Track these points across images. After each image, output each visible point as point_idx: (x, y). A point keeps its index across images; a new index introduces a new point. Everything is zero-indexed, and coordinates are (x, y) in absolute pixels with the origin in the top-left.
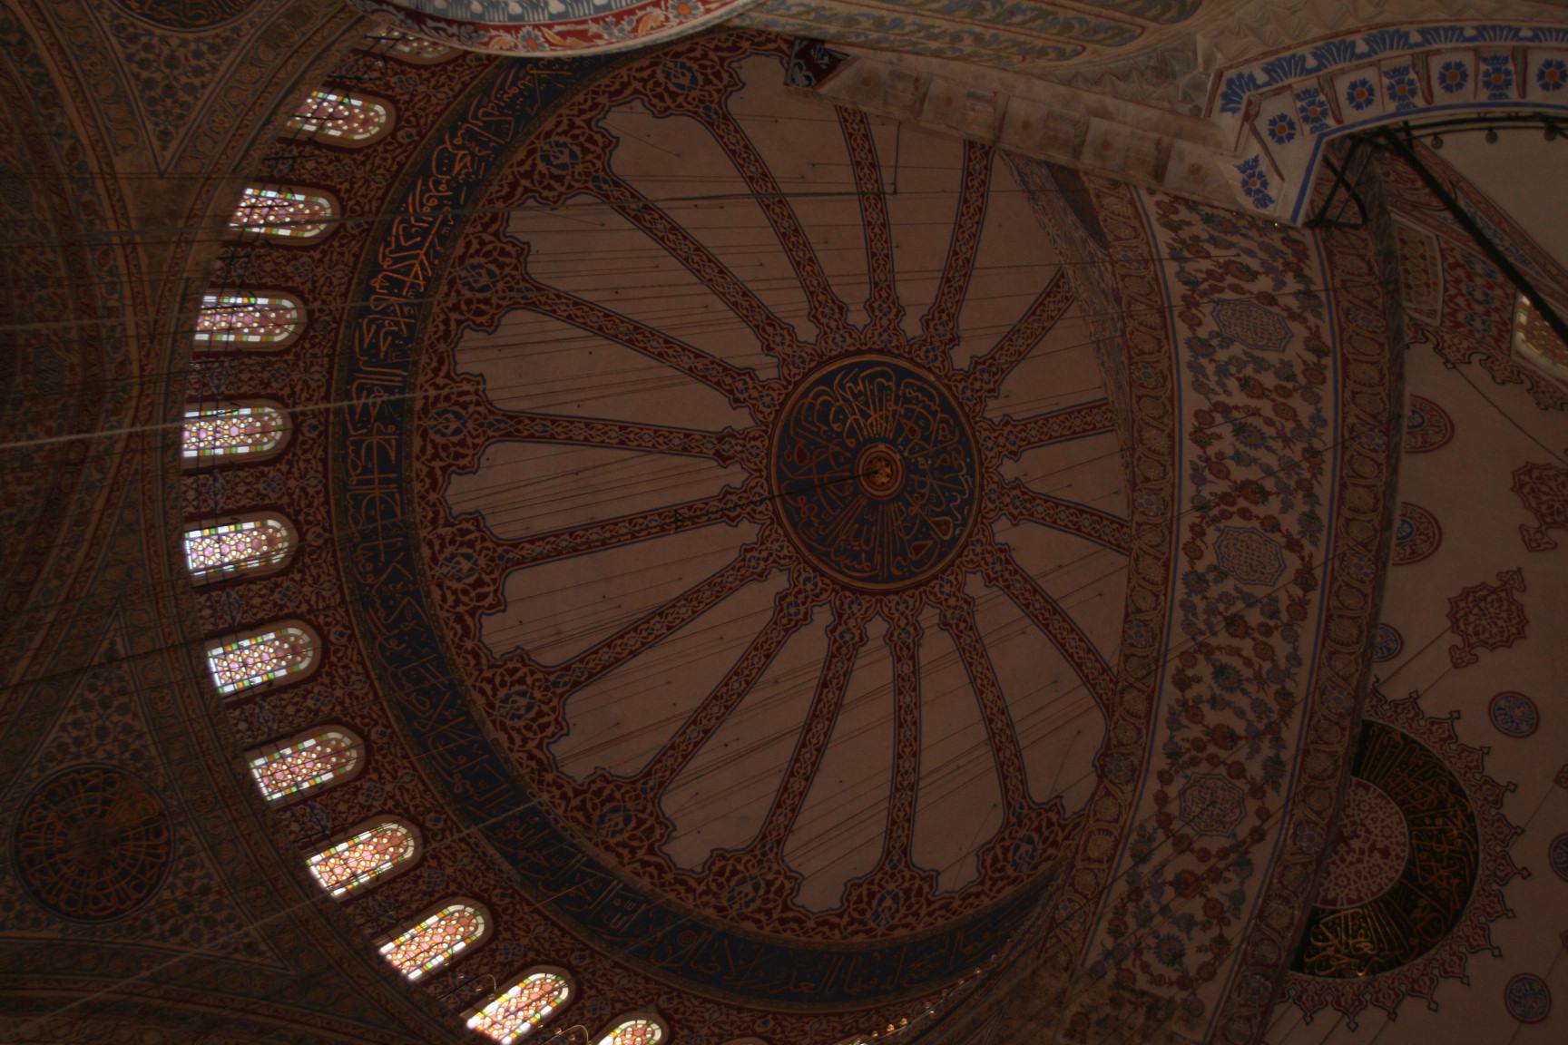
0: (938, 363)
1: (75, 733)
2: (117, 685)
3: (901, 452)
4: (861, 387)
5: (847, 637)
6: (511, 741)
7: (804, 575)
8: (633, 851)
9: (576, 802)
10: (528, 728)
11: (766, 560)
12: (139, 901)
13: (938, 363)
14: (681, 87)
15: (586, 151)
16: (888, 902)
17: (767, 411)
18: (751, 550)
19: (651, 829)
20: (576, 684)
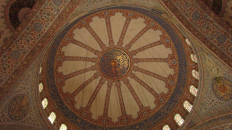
1: (21, 88)
2: (28, 81)
5: (102, 82)
6: (58, 85)
8: (71, 105)
9: (64, 96)
10: (60, 84)
12: (24, 117)
14: (129, 15)
15: (110, 14)
16: (104, 121)
19: (73, 102)
20: (67, 78)
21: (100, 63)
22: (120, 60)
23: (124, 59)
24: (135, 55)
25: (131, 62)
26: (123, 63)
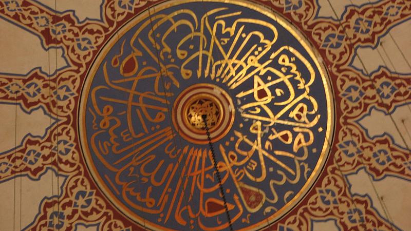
0: (337, 52)
3: (237, 106)
4: (232, 30)
7: (80, 188)
11: (45, 158)
13: (337, 52)
17: (119, 10)
18: (35, 143)
21: (88, 116)
22: (249, 84)
23: (285, 79)
24: (372, 41)
25: (337, 100)
26: (276, 110)
